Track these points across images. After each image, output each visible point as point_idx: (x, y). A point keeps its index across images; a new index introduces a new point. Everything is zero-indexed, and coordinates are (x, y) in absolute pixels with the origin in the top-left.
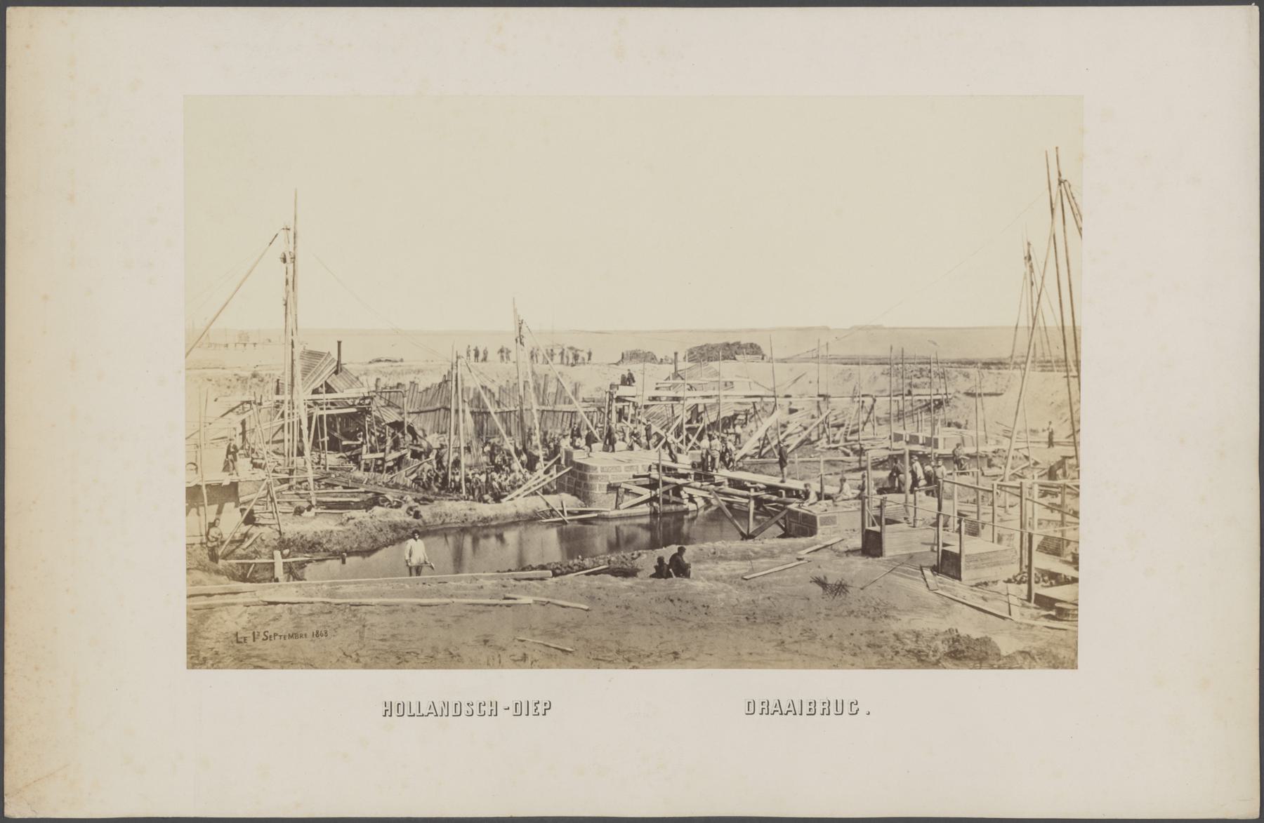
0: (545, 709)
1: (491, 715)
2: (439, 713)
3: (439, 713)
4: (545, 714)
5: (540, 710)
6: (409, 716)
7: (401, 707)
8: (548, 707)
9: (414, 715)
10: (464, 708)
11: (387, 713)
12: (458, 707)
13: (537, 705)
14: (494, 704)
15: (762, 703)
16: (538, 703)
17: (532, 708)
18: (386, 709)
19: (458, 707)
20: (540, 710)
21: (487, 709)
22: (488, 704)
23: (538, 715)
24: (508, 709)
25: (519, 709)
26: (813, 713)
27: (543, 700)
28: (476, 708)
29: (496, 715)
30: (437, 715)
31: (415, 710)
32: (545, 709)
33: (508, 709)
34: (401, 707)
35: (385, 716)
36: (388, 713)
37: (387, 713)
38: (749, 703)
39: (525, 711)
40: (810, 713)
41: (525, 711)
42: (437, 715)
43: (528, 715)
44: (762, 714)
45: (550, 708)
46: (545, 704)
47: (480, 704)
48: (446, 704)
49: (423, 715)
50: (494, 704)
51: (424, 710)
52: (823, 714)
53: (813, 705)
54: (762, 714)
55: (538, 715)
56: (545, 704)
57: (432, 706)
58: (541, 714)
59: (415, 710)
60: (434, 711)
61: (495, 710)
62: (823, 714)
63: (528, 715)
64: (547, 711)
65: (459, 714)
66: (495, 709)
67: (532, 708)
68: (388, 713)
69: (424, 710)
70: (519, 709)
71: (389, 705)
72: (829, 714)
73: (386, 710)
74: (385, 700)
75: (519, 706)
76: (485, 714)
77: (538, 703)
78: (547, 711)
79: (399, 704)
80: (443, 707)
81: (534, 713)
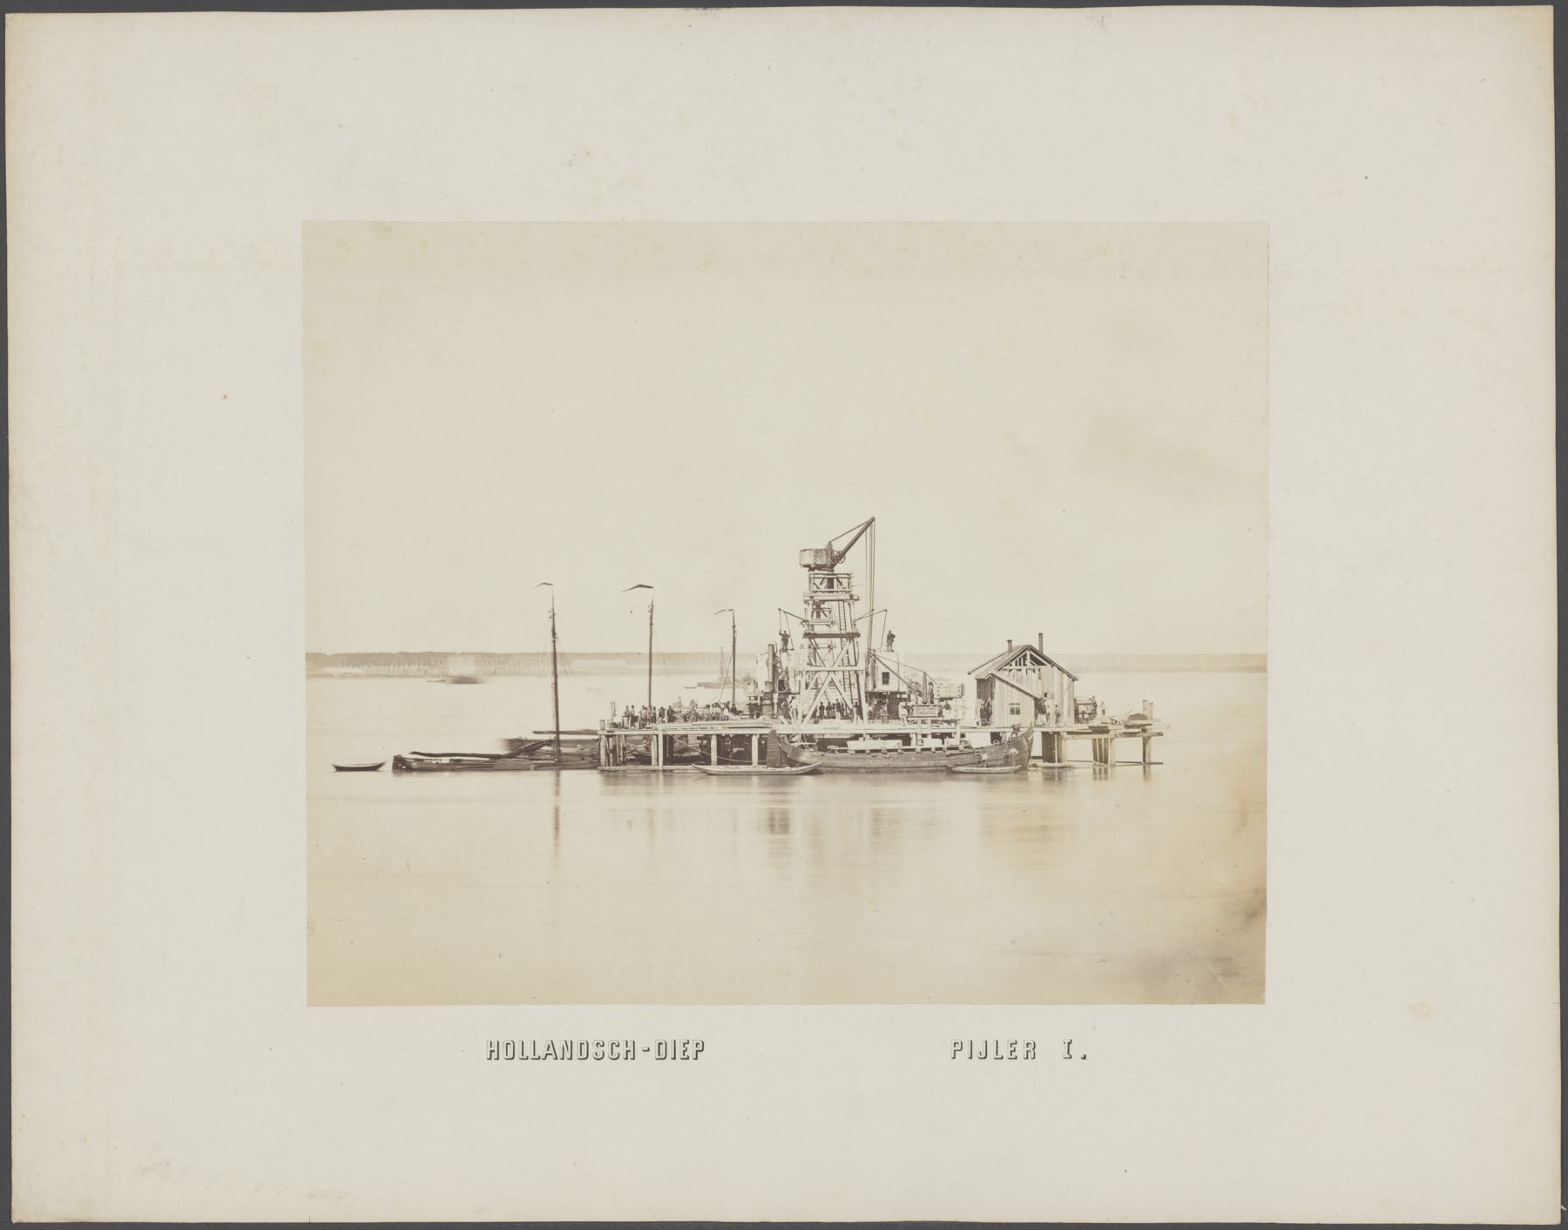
0: (697, 1051)
2: (560, 1055)
3: (560, 1055)
4: (696, 1059)
7: (510, 1048)
10: (592, 1049)
11: (493, 1054)
12: (584, 1047)
13: (686, 1045)
14: (631, 1044)
15: (1028, 1044)
16: (688, 1043)
17: (680, 1049)
18: (492, 1049)
19: (584, 1047)
20: (691, 1052)
21: (622, 1050)
22: (623, 1045)
23: (688, 1058)
25: (662, 1051)
27: (695, 1037)
28: (607, 1049)
29: (633, 1059)
30: (556, 1059)
31: (528, 1052)
32: (697, 1051)
33: (648, 1050)
34: (510, 1048)
36: (494, 1055)
37: (493, 1054)
38: (581, 1044)
39: (670, 1054)
41: (670, 1054)
42: (556, 1059)
44: (490, 1059)
45: (702, 1050)
46: (697, 1044)
47: (613, 1044)
48: (569, 1046)
49: (539, 1058)
50: (631, 1044)
52: (627, 1059)
53: (1031, 1048)
55: (688, 1058)
56: (697, 1044)
57: (551, 1045)
59: (528, 1052)
60: (551, 1051)
61: (632, 1051)
62: (627, 1059)
63: (675, 1058)
66: (632, 1049)
67: (680, 1049)
68: (494, 1055)
69: (541, 1051)
70: (662, 1051)
71: (495, 1044)
72: (498, 1059)
75: (663, 1047)
76: (588, 1056)
77: (688, 1043)
81: (683, 1057)
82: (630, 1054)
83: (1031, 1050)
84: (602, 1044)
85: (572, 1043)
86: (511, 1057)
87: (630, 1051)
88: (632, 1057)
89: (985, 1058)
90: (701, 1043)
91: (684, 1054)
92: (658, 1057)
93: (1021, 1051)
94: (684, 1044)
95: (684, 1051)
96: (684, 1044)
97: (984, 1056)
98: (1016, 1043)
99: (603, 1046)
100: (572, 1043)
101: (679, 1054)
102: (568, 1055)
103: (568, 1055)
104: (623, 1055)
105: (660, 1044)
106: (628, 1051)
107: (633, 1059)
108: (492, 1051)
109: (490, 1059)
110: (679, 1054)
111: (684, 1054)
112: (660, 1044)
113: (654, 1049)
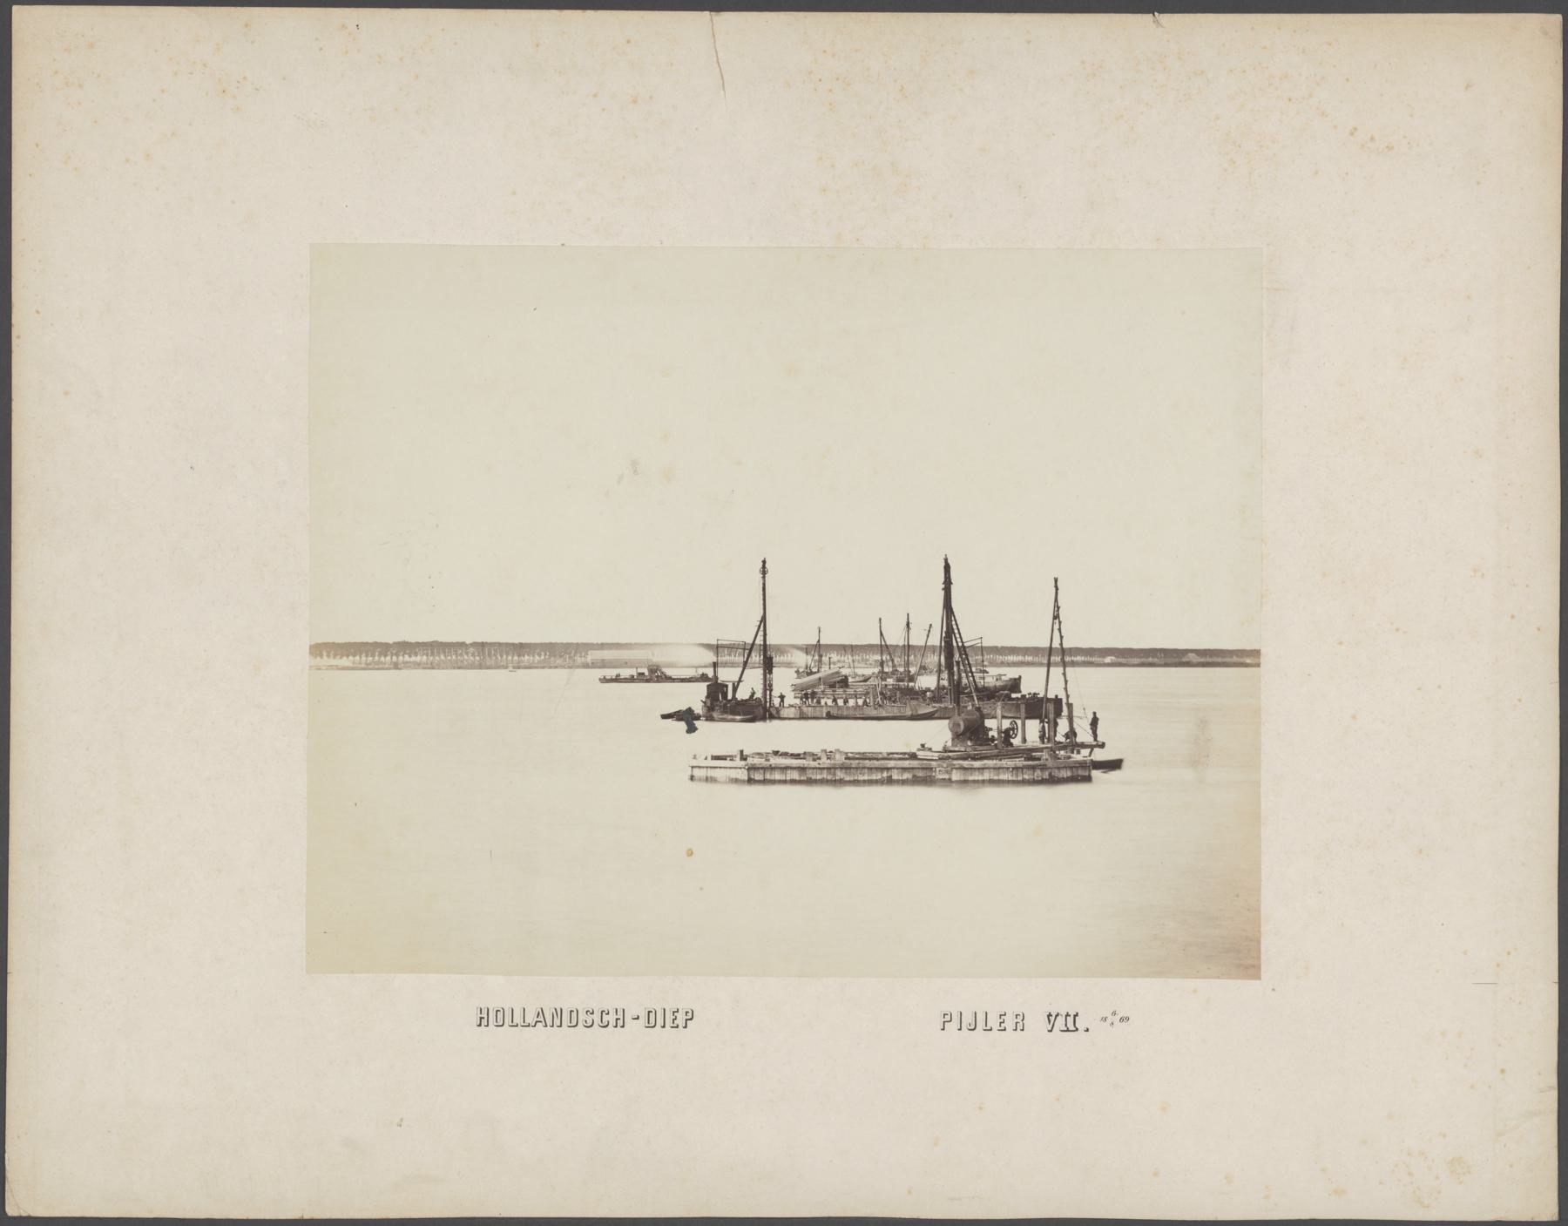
0: (687, 1020)
1: (616, 1027)
2: (549, 1022)
3: (549, 1022)
4: (686, 1027)
5: (680, 1021)
7: (500, 1015)
8: (690, 1016)
9: (517, 1026)
10: (582, 1017)
12: (574, 1014)
13: (676, 1014)
15: (1017, 1015)
16: (678, 1011)
17: (669, 1017)
19: (574, 1014)
20: (680, 1021)
21: (611, 1018)
22: (612, 1012)
23: (677, 1027)
24: (638, 1018)
25: (651, 1019)
26: (501, 1024)
27: (683, 1007)
28: (596, 1017)
29: (623, 1026)
31: (518, 1019)
32: (687, 1020)
33: (638, 1018)
34: (500, 1015)
35: (480, 1025)
36: (484, 1022)
38: (571, 1011)
39: (660, 1022)
41: (660, 1022)
43: (664, 1027)
45: (691, 1019)
46: (687, 1013)
48: (558, 1013)
50: (620, 1013)
53: (1020, 1018)
54: (1016, 1030)
55: (677, 1027)
56: (687, 1013)
58: (680, 1027)
59: (518, 1019)
60: (542, 1019)
63: (664, 1027)
64: (688, 1022)
65: (575, 1024)
67: (669, 1017)
69: (530, 1019)
70: (651, 1019)
71: (484, 1012)
72: (488, 1026)
73: (617, 1019)
75: (652, 1015)
77: (678, 1011)
78: (688, 1022)
79: (497, 1011)
82: (620, 1023)
83: (1020, 1024)
84: (591, 1011)
85: (561, 1010)
88: (622, 1024)
89: (975, 1029)
90: (691, 1012)
91: (673, 1023)
92: (647, 1025)
93: (1009, 1024)
94: (674, 1012)
95: (674, 1020)
96: (674, 1012)
97: (973, 1027)
98: (1005, 1015)
99: (592, 1013)
100: (561, 1010)
101: (669, 1023)
102: (557, 1022)
103: (557, 1022)
104: (612, 1023)
105: (649, 1012)
106: (617, 1019)
107: (623, 1026)
108: (481, 1018)
110: (669, 1023)
111: (673, 1023)
112: (649, 1012)
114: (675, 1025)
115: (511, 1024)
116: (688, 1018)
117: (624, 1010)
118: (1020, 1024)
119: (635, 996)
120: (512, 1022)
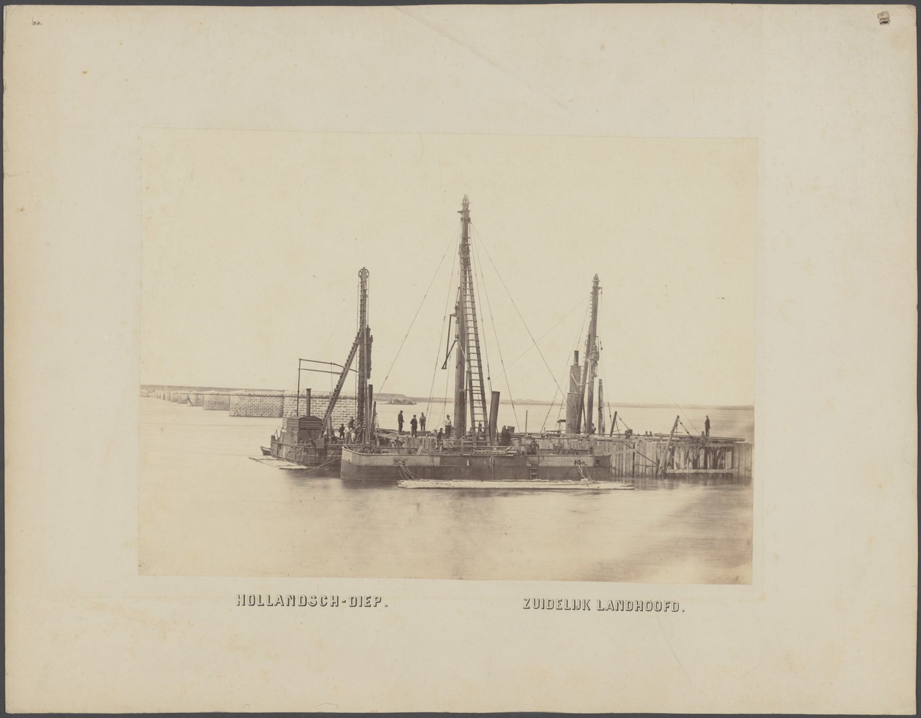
0: (376, 603)
5: (373, 602)
6: (268, 605)
7: (252, 599)
16: (370, 598)
20: (373, 602)
24: (345, 602)
25: (354, 602)
30: (283, 605)
32: (376, 603)
33: (345, 602)
34: (252, 599)
39: (359, 603)
40: (260, 604)
41: (359, 603)
42: (283, 605)
43: (361, 606)
44: (239, 605)
49: (272, 605)
51: (273, 601)
58: (372, 606)
59: (264, 600)
60: (281, 602)
65: (304, 604)
69: (273, 601)
70: (354, 602)
71: (242, 597)
74: (333, 595)
75: (354, 600)
76: (306, 604)
80: (290, 598)
85: (294, 597)
86: (253, 604)
87: (335, 603)
99: (316, 598)
105: (352, 598)
109: (239, 605)
110: (364, 603)
112: (352, 598)
113: (348, 602)
114: (369, 604)
115: (259, 604)
116: (377, 601)
117: (338, 597)
118: (587, 607)
119: (346, 588)
120: (260, 602)
